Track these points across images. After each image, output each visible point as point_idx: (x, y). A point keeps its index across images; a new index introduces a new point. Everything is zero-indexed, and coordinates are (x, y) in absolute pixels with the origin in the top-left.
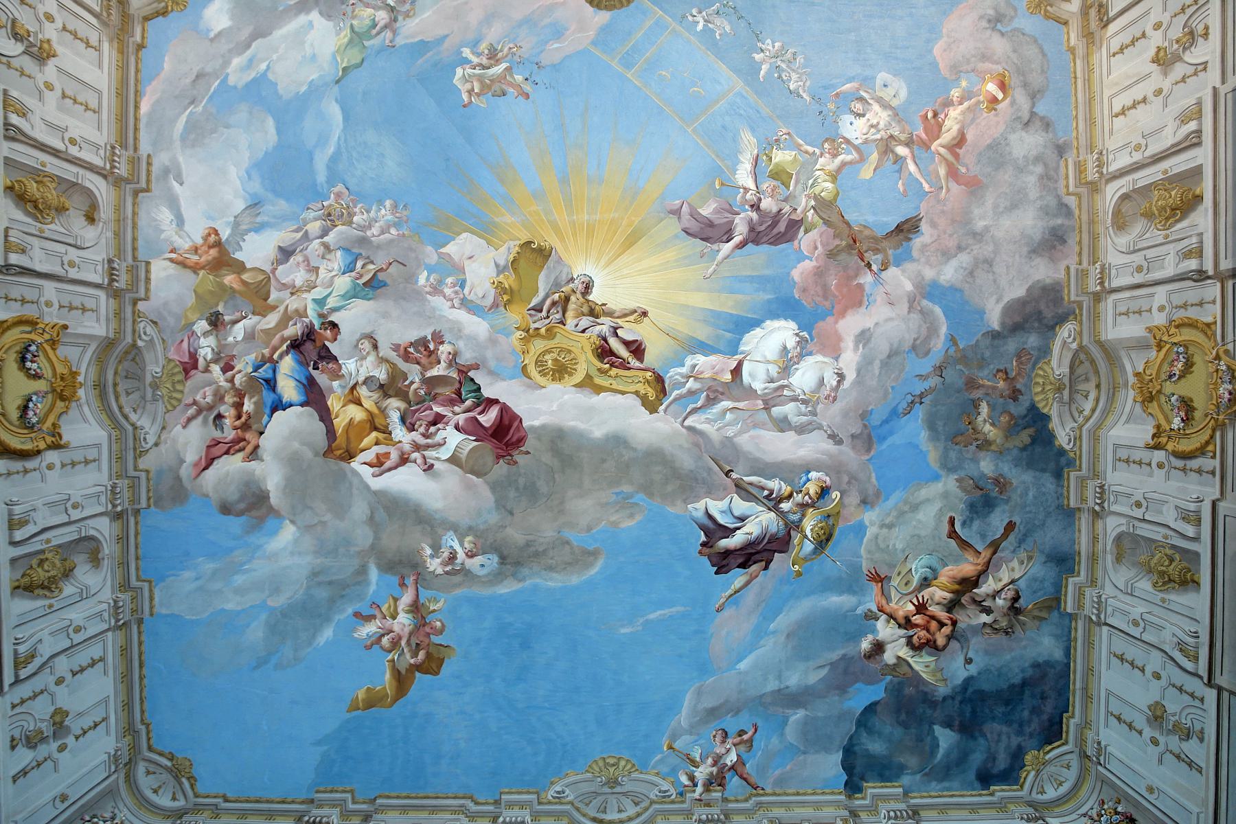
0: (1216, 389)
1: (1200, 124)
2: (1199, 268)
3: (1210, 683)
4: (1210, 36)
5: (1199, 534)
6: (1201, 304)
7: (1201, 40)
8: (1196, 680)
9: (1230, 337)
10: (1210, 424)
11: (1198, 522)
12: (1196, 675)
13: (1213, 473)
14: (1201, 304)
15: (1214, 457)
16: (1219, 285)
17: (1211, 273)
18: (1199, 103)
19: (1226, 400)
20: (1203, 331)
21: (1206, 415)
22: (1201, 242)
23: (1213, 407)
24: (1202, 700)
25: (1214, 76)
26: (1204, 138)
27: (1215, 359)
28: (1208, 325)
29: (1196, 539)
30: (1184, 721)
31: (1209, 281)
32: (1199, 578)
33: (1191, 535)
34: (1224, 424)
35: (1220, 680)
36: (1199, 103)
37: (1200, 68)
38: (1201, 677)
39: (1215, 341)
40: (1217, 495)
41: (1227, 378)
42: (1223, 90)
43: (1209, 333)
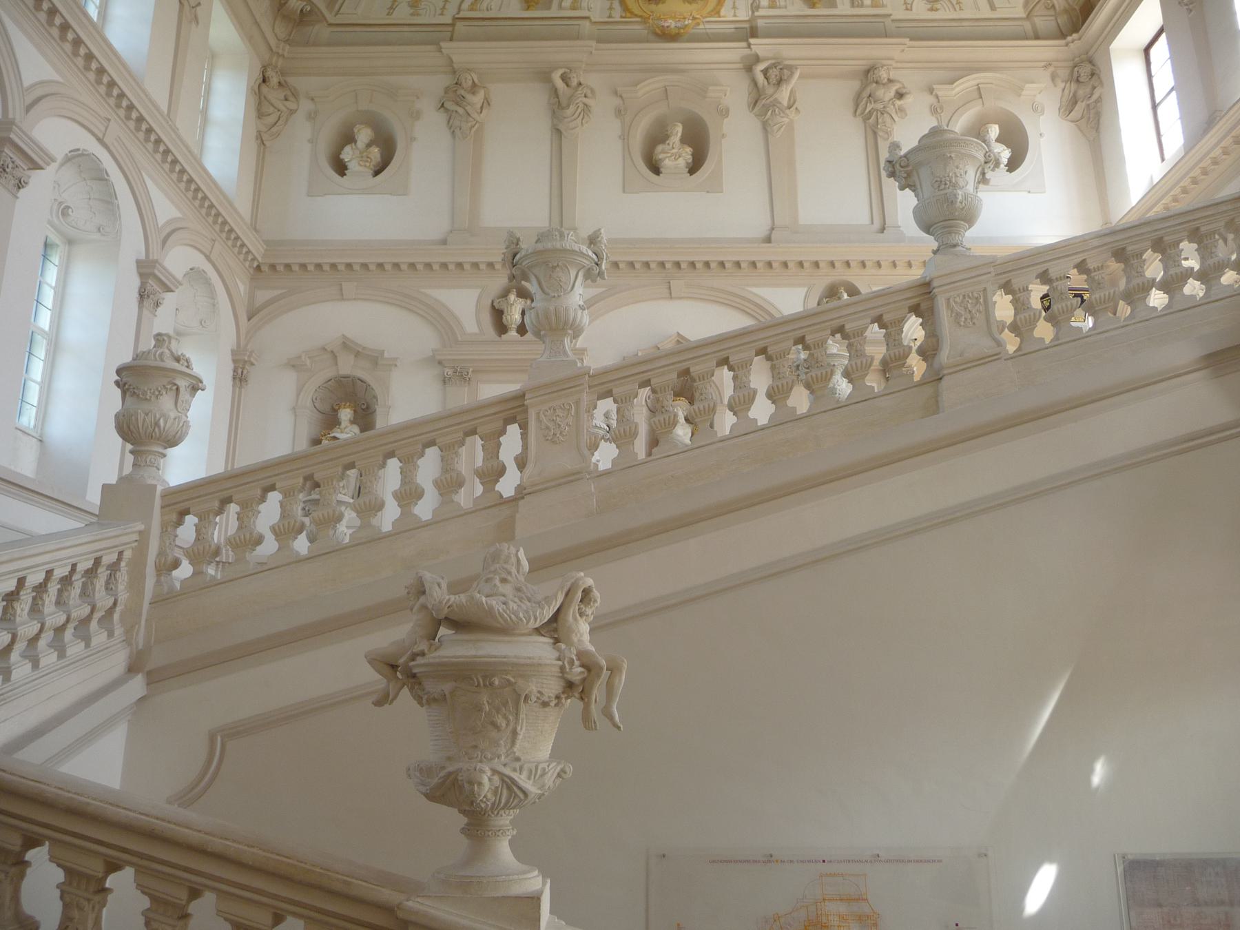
0: (672, 18)
1: (867, 7)
2: (761, 6)
3: (455, 19)
4: (929, 12)
5: (565, 9)
6: (734, 7)
7: (929, 6)
8: (456, 11)
9: (708, 26)
10: (644, 14)
11: (573, 8)
12: (459, 10)
13: (610, 17)
14: (734, 7)
15: (622, 17)
16: (747, 19)
17: (756, 14)
18: (883, 6)
19: (663, 24)
20: (715, 9)
21: (652, 12)
22: (780, 8)
23: (658, 15)
24: (442, 14)
25: (900, 14)
26: (857, 9)
27: (693, 17)
28: (718, 14)
29: (560, 7)
30: (423, 3)
31: (750, 13)
32: (532, 10)
33: (563, 4)
34: (645, 23)
35: (459, 25)
36: (883, 6)
37: (909, 6)
38: (458, 13)
39: (706, 17)
40: (593, 20)
41: (679, 25)
42: (888, 21)
43: (713, 13)
